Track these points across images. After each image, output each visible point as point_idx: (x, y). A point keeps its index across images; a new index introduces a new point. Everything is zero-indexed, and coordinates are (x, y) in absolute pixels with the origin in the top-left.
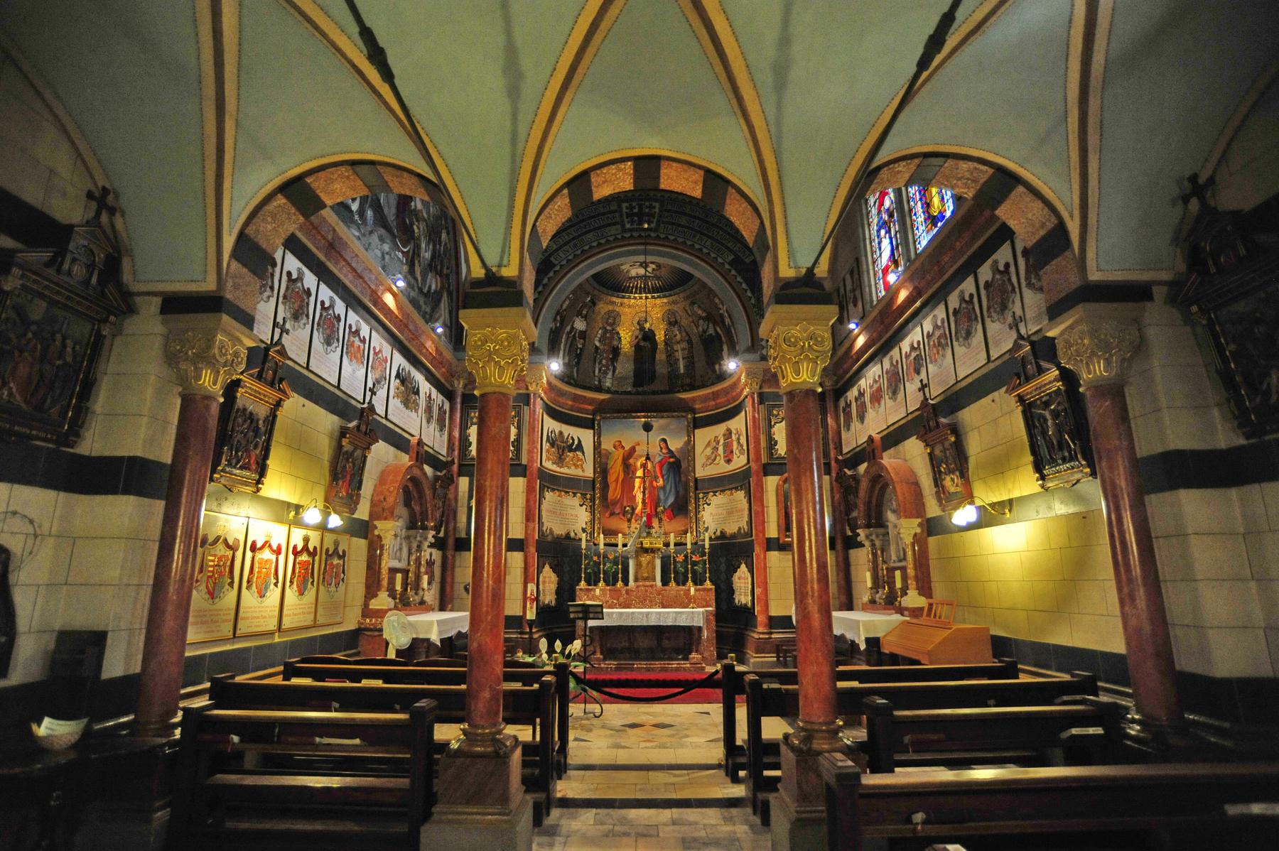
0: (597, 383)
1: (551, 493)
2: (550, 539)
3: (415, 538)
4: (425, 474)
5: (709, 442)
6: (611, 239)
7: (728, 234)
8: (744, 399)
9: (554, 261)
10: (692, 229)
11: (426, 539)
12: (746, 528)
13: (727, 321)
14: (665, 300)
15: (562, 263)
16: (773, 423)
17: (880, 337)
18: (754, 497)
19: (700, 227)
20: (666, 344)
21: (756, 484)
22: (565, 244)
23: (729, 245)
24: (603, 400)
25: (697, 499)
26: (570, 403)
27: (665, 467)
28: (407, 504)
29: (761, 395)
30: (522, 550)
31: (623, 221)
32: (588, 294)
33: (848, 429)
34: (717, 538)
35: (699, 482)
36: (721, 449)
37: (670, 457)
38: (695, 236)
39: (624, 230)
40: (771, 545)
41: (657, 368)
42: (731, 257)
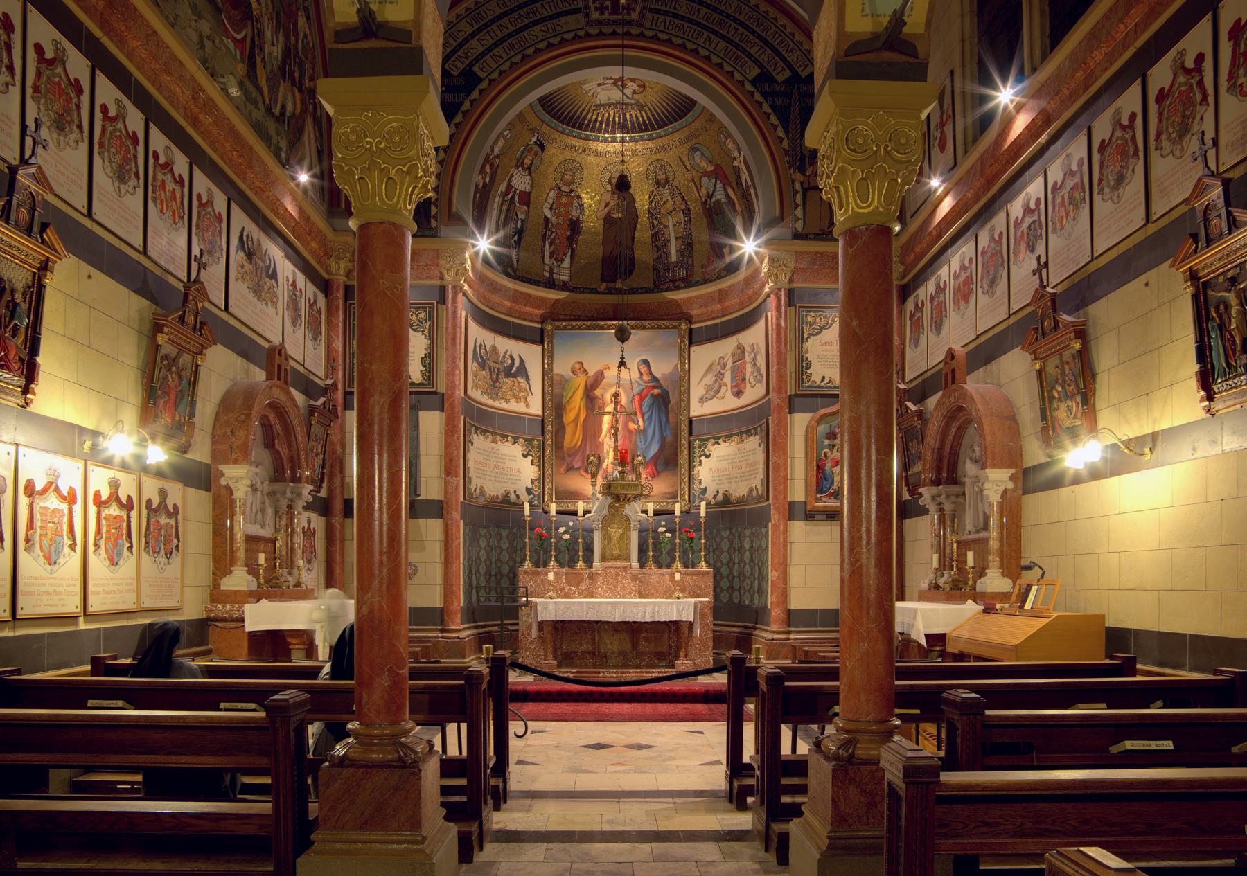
0: (547, 274)
1: (481, 437)
2: (481, 501)
3: (284, 493)
4: (293, 399)
5: (712, 365)
7: (753, 32)
8: (765, 300)
9: (479, 73)
10: (698, 24)
11: (299, 495)
12: (760, 488)
13: (745, 177)
14: (650, 144)
15: (492, 77)
16: (806, 336)
17: (977, 198)
18: (774, 444)
19: (708, 20)
20: (651, 215)
21: (778, 425)
22: (496, 45)
23: (753, 51)
24: (557, 301)
25: (690, 448)
26: (508, 303)
27: (647, 401)
28: (269, 444)
29: (790, 293)
30: (441, 516)
31: (586, 7)
32: (533, 131)
33: (916, 345)
34: (718, 504)
35: (694, 423)
36: (727, 378)
37: (655, 387)
38: (699, 35)
39: (589, 23)
40: (793, 511)
41: (637, 253)
42: (756, 71)
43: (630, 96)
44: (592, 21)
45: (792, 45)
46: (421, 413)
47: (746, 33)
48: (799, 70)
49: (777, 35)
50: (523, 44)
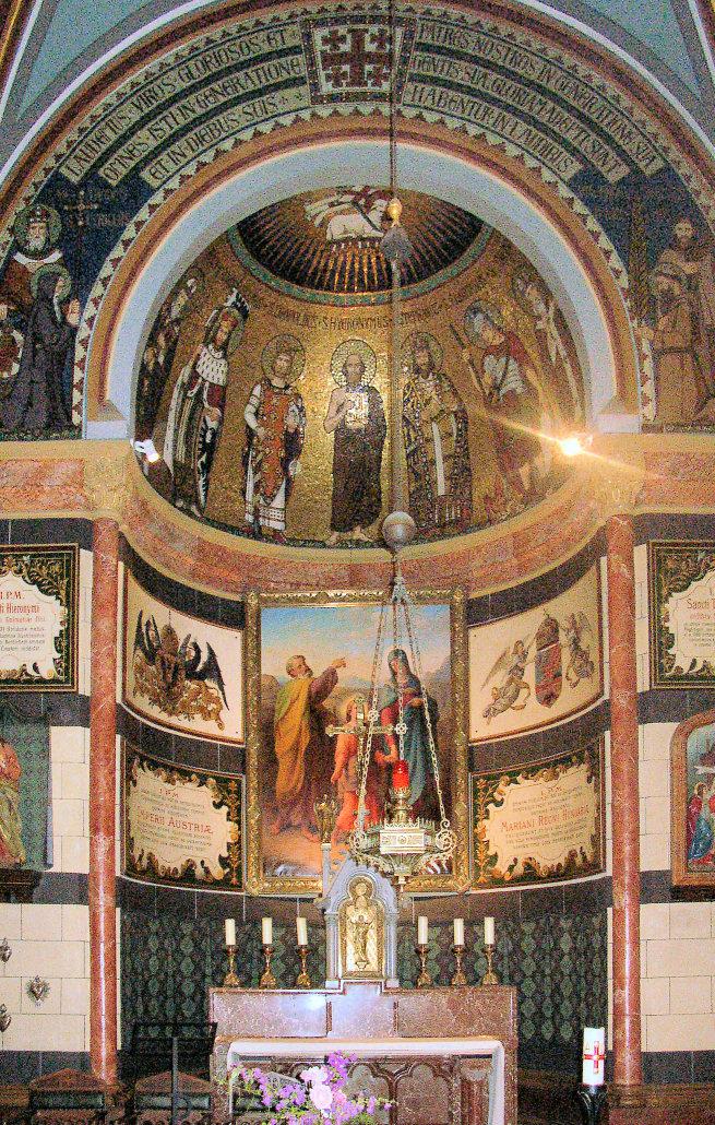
6: (287, 121)
22: (174, 138)
23: (569, 136)
31: (314, 75)
39: (317, 100)
43: (378, 225)
44: (322, 96)
45: (629, 127)
46: (53, 729)
47: (558, 109)
48: (642, 165)
49: (605, 113)
50: (217, 134)
